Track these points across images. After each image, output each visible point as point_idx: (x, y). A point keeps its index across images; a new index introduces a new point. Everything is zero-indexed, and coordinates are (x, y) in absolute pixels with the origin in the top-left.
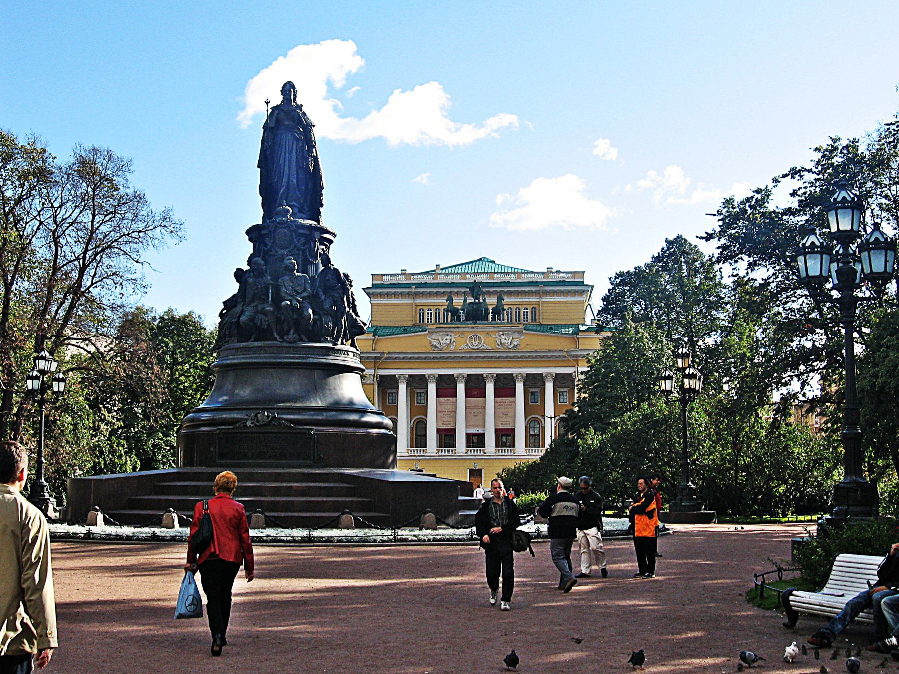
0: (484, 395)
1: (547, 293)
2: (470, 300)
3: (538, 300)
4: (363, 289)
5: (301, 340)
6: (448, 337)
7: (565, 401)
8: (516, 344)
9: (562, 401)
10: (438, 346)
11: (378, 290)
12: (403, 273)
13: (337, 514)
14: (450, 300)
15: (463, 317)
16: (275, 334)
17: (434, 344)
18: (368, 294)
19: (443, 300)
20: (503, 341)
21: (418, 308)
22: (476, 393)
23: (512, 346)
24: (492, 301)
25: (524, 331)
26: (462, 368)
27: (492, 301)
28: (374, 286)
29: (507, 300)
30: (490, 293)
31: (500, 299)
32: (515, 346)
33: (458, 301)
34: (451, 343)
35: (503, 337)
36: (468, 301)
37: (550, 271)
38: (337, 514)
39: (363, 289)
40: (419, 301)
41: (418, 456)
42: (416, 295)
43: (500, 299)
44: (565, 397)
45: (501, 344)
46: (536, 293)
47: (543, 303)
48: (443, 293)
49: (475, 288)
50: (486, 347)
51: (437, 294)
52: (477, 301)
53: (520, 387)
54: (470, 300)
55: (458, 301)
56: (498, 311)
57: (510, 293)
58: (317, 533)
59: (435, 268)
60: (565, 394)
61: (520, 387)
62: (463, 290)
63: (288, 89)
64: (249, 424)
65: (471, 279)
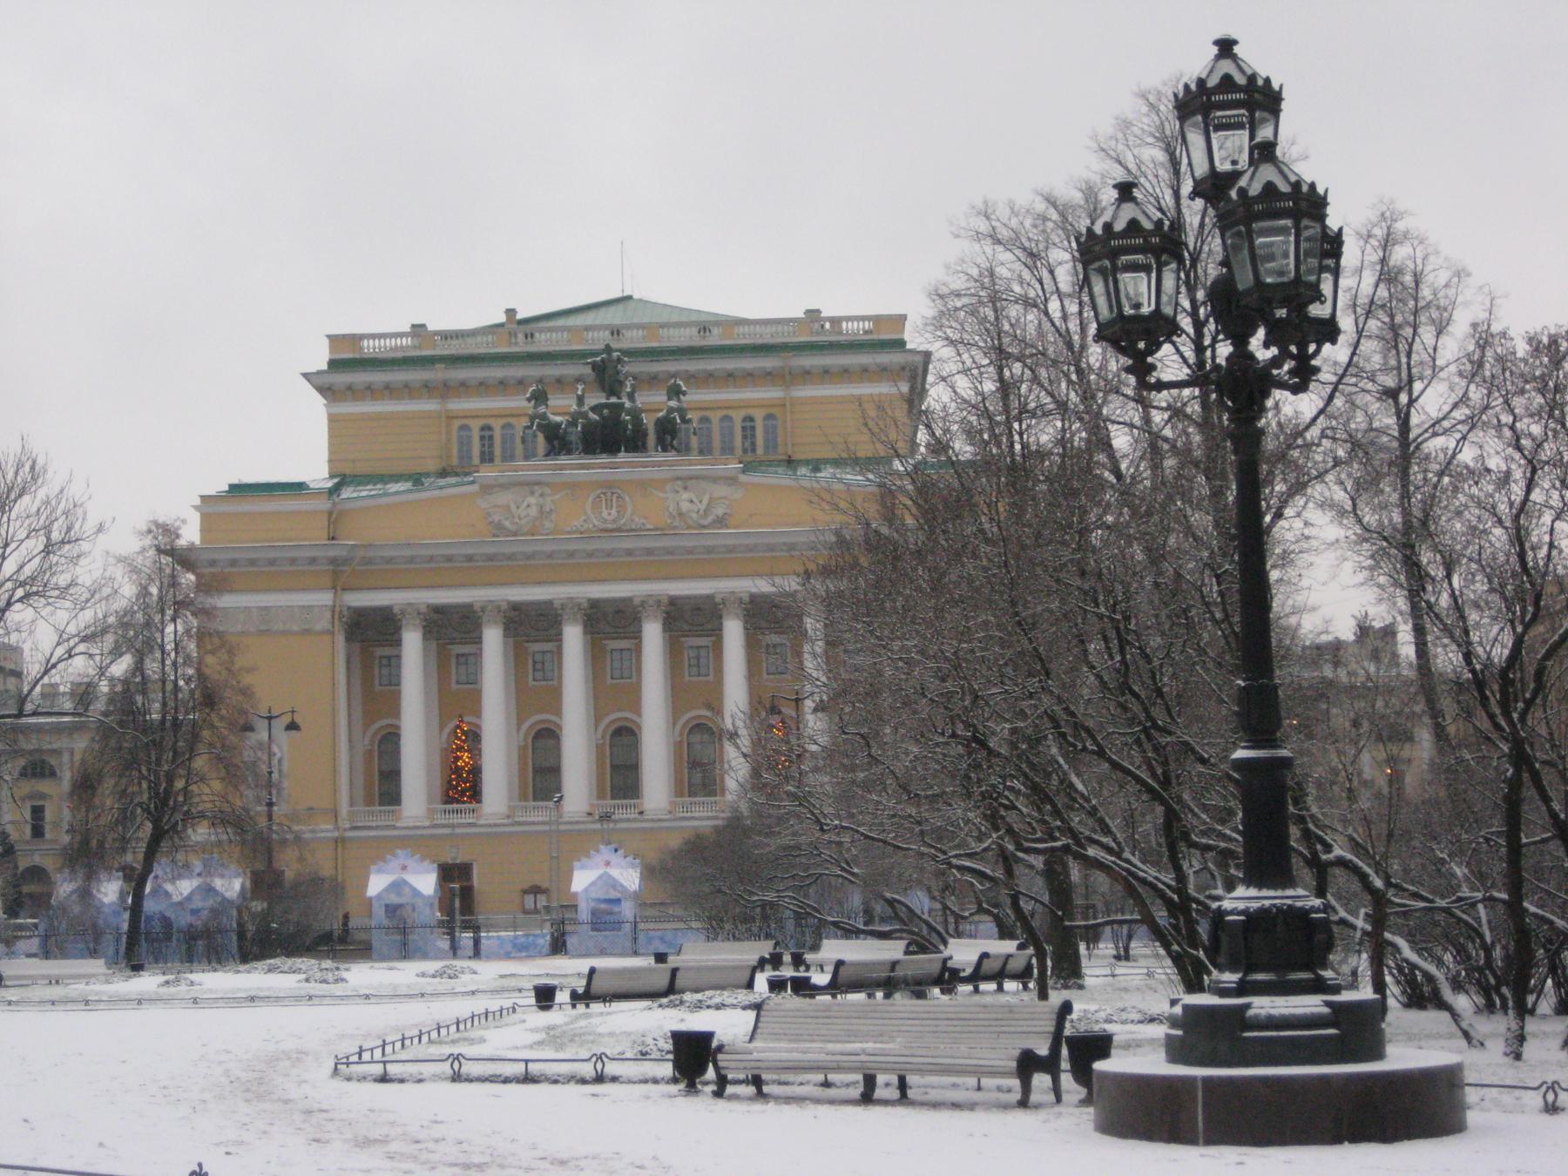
1: (806, 376)
2: (596, 398)
4: (305, 375)
6: (532, 500)
8: (720, 511)
10: (507, 524)
12: (418, 330)
17: (496, 518)
18: (323, 390)
19: (519, 403)
20: (685, 506)
21: (457, 423)
23: (710, 519)
24: (651, 403)
28: (334, 364)
29: (694, 396)
30: (653, 380)
35: (685, 496)
37: (813, 315)
39: (305, 375)
42: (445, 390)
45: (681, 514)
46: (770, 377)
48: (521, 383)
51: (503, 386)
54: (596, 398)
57: (709, 379)
65: (598, 340)
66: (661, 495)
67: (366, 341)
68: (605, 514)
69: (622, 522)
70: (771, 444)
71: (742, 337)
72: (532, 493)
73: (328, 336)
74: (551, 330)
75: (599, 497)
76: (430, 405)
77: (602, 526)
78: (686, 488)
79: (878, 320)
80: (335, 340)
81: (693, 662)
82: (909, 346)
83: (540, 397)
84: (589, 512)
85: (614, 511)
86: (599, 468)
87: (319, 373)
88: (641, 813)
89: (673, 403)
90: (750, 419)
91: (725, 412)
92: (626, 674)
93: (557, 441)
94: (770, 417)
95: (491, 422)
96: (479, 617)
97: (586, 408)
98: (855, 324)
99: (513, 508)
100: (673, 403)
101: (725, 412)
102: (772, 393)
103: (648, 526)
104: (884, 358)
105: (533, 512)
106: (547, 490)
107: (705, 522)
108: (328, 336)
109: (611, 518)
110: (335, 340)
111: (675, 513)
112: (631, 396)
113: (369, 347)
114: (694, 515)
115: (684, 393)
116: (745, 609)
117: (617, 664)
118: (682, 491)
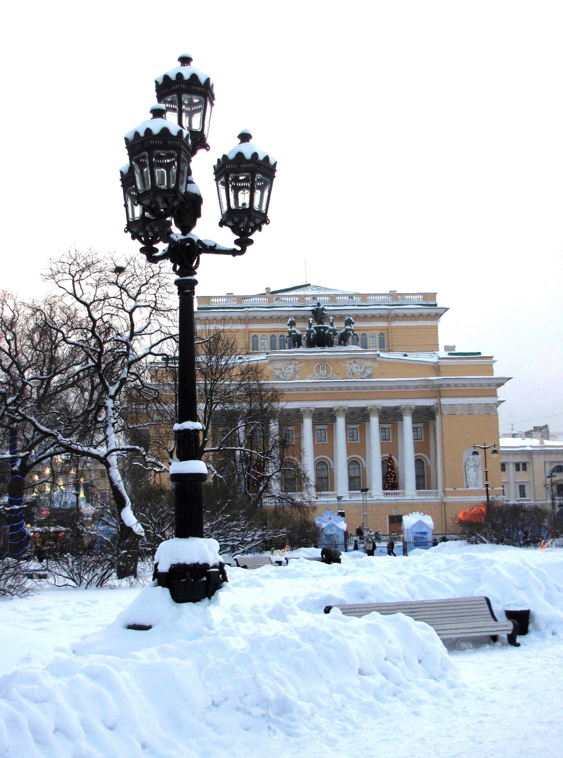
6: (291, 367)
7: (419, 437)
19: (285, 326)
20: (355, 370)
23: (365, 375)
35: (355, 365)
40: (252, 327)
44: (419, 434)
47: (393, 328)
59: (265, 292)
60: (419, 430)
66: (344, 365)
67: (213, 299)
68: (321, 373)
69: (329, 376)
72: (291, 364)
74: (286, 296)
78: (355, 362)
81: (351, 435)
85: (325, 371)
86: (318, 352)
89: (348, 327)
91: (363, 332)
92: (355, 438)
93: (296, 341)
94: (381, 334)
97: (312, 329)
99: (283, 369)
100: (348, 327)
101: (363, 332)
102: (383, 324)
105: (292, 371)
106: (297, 362)
107: (363, 377)
109: (324, 374)
112: (332, 324)
114: (359, 374)
115: (353, 323)
117: (319, 436)
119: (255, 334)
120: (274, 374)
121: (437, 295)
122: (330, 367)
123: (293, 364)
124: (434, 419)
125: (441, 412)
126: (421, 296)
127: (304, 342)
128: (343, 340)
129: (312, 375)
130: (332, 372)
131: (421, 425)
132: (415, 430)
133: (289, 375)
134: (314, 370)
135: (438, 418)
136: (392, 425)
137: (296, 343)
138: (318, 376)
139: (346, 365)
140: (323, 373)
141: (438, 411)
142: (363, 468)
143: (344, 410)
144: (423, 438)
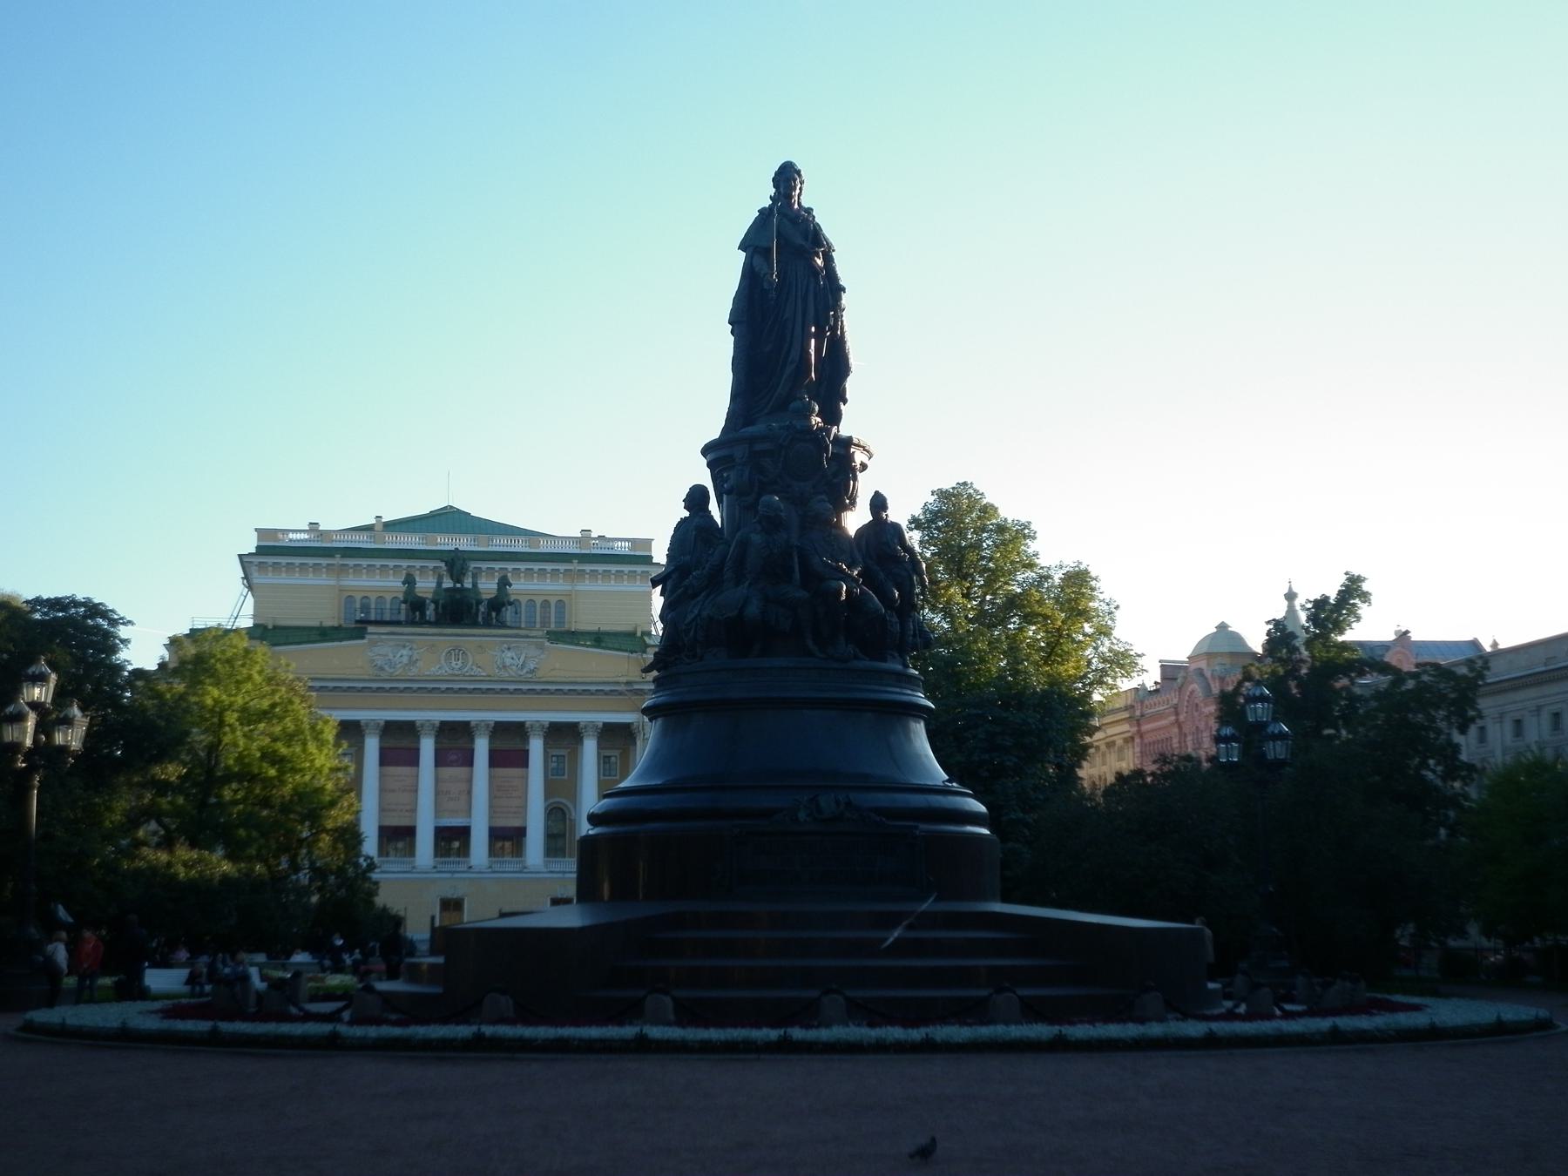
0: (469, 761)
3: (569, 588)
5: (856, 657)
6: (405, 652)
8: (532, 666)
9: (607, 773)
10: (386, 667)
11: (270, 560)
13: (814, 993)
14: (410, 581)
15: (430, 612)
16: (810, 643)
17: (379, 663)
20: (508, 662)
22: (454, 757)
23: (525, 671)
25: (547, 644)
26: (431, 710)
27: (488, 587)
28: (262, 550)
31: (504, 583)
32: (532, 671)
33: (426, 585)
34: (412, 662)
36: (445, 586)
38: (814, 993)
41: (398, 872)
43: (504, 583)
45: (504, 667)
49: (455, 563)
50: (476, 671)
52: (458, 585)
53: (536, 747)
54: (448, 583)
55: (426, 585)
56: (498, 604)
58: (226, 1027)
60: (613, 759)
61: (536, 747)
62: (431, 564)
63: (786, 177)
64: (802, 815)
69: (466, 670)
70: (560, 620)
71: (545, 547)
72: (404, 647)
73: (256, 530)
75: (449, 652)
76: (324, 580)
77: (450, 672)
78: (509, 649)
79: (633, 541)
80: (261, 532)
82: (654, 561)
83: (410, 581)
84: (443, 662)
85: (459, 662)
87: (250, 554)
88: (470, 867)
90: (546, 604)
95: (368, 594)
96: (364, 731)
98: (620, 543)
103: (484, 674)
104: (639, 569)
105: (405, 660)
108: (256, 530)
109: (458, 667)
110: (261, 532)
111: (501, 666)
113: (285, 541)
114: (514, 667)
116: (545, 732)
118: (506, 651)
119: (350, 593)
120: (375, 663)
121: (653, 543)
122: (469, 654)
123: (408, 648)
124: (635, 744)
125: (644, 735)
126: (627, 543)
127: (430, 612)
128: (494, 610)
129: (437, 667)
130: (470, 664)
131: (617, 753)
132: (604, 761)
133: (400, 665)
134: (443, 658)
135: (639, 743)
136: (569, 750)
137: (417, 613)
138: (447, 669)
139: (495, 653)
140: (457, 664)
141: (639, 732)
142: (570, 820)
143: (488, 726)
144: (618, 774)
